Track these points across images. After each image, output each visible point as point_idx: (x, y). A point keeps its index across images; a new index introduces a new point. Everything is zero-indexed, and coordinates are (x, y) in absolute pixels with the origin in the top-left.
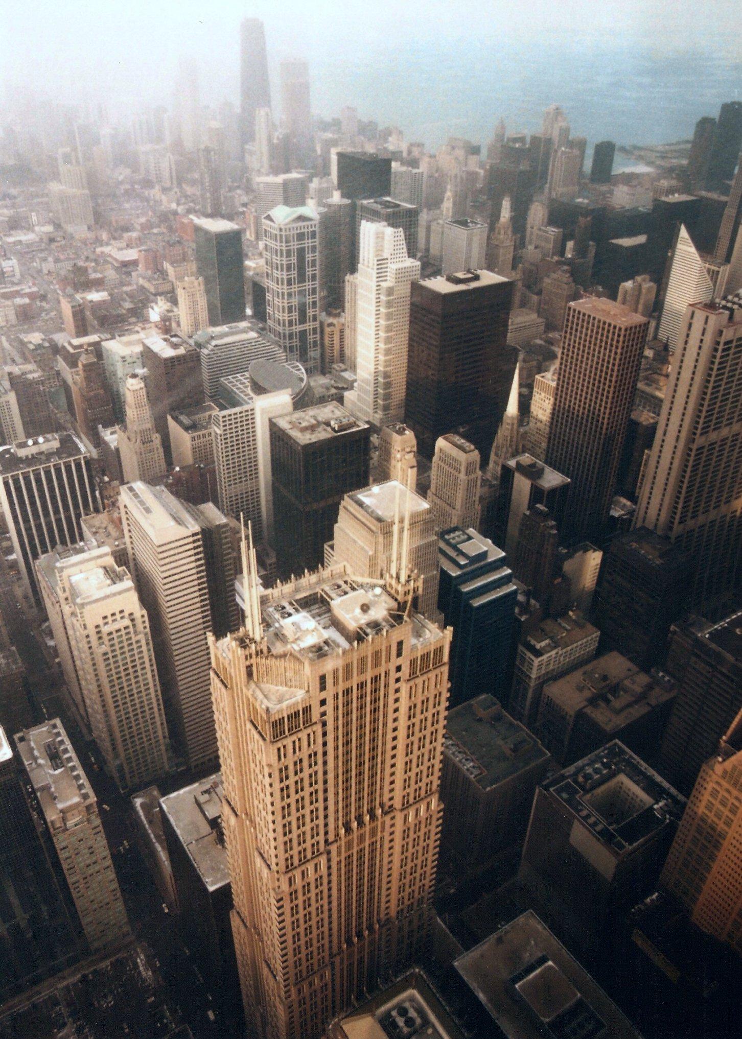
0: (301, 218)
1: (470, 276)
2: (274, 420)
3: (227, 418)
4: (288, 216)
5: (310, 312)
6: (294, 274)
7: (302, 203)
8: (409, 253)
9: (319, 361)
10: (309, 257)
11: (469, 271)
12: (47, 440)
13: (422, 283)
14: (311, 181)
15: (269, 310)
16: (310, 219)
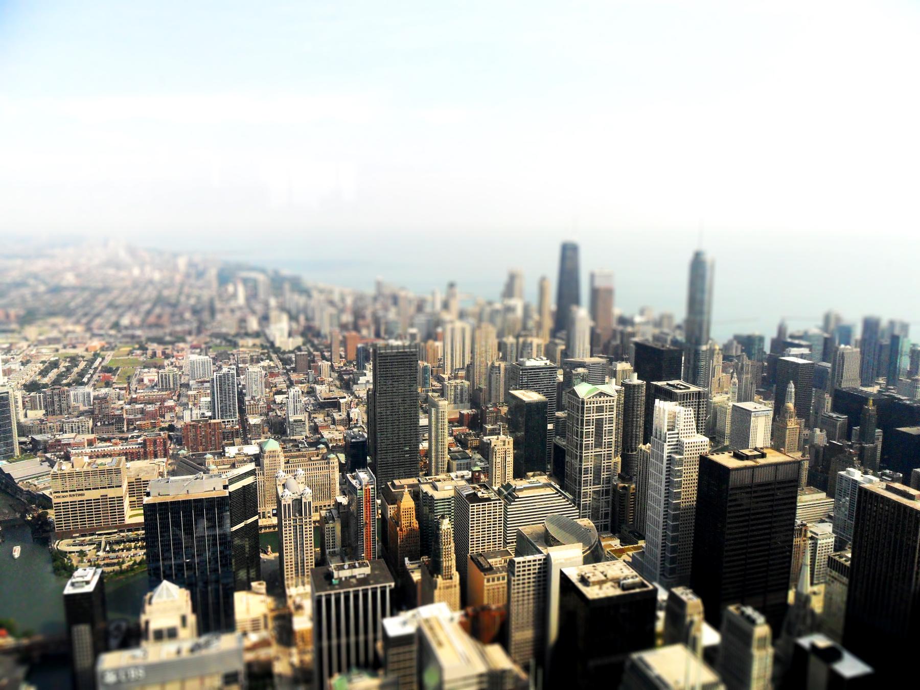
0: (601, 394)
1: (756, 453)
2: (564, 570)
3: (522, 565)
4: (589, 392)
5: (604, 475)
6: (591, 441)
7: (603, 383)
8: (697, 429)
9: (609, 520)
10: (606, 427)
11: (756, 449)
12: (361, 565)
13: (710, 457)
14: (611, 364)
15: (568, 470)
16: (608, 395)
